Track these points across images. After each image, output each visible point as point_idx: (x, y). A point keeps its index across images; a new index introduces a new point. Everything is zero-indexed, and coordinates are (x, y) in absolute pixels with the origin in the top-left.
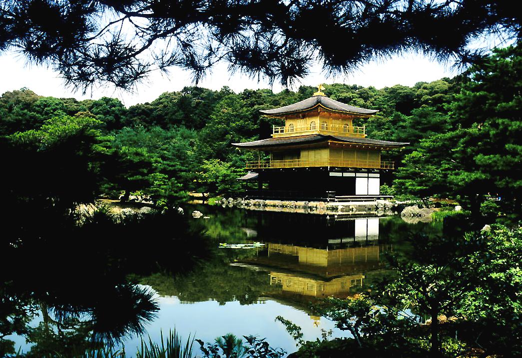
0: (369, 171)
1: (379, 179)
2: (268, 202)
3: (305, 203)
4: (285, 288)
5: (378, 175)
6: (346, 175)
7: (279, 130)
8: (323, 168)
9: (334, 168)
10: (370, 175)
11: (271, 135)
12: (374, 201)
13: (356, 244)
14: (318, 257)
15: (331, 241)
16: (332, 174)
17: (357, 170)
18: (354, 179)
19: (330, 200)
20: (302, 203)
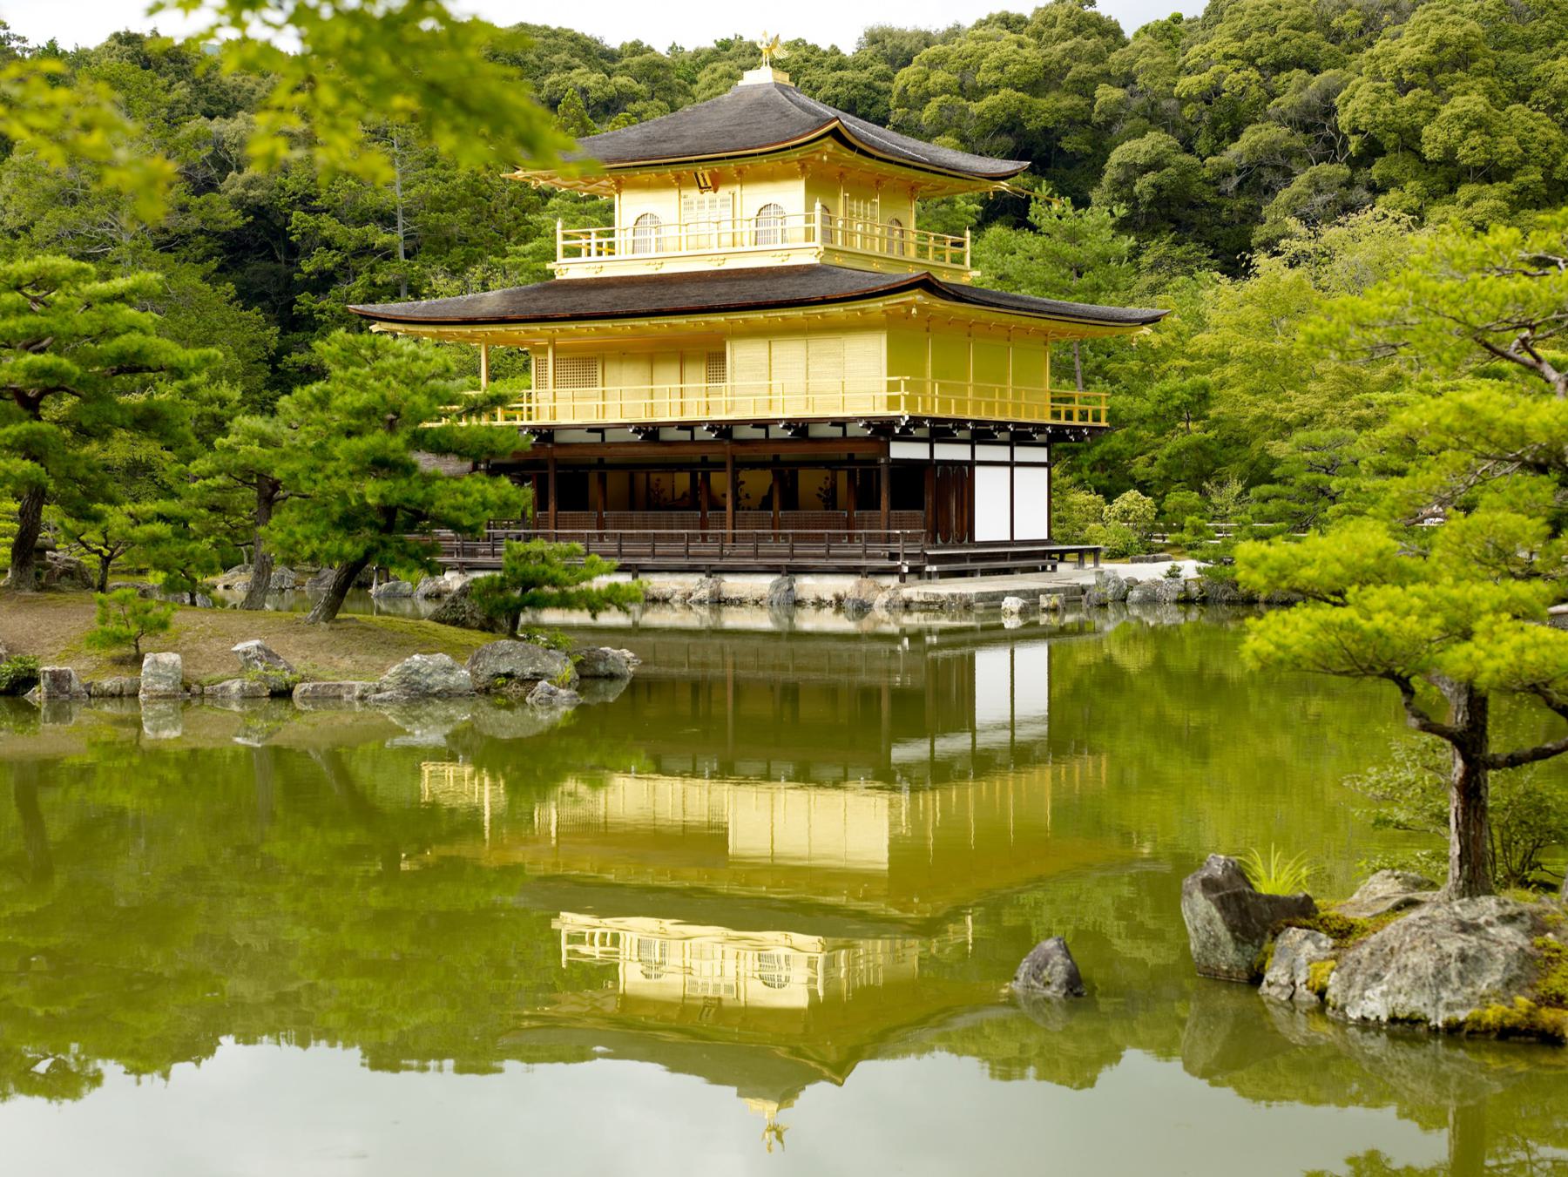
0: (1021, 435)
1: (1045, 470)
3: (776, 587)
4: (632, 977)
5: (1040, 455)
6: (944, 452)
7: (594, 240)
8: (869, 422)
10: (1022, 454)
11: (550, 266)
12: (1044, 569)
13: (982, 763)
14: (841, 825)
15: (901, 753)
16: (899, 451)
17: (983, 433)
18: (972, 464)
19: (912, 570)
20: (763, 584)
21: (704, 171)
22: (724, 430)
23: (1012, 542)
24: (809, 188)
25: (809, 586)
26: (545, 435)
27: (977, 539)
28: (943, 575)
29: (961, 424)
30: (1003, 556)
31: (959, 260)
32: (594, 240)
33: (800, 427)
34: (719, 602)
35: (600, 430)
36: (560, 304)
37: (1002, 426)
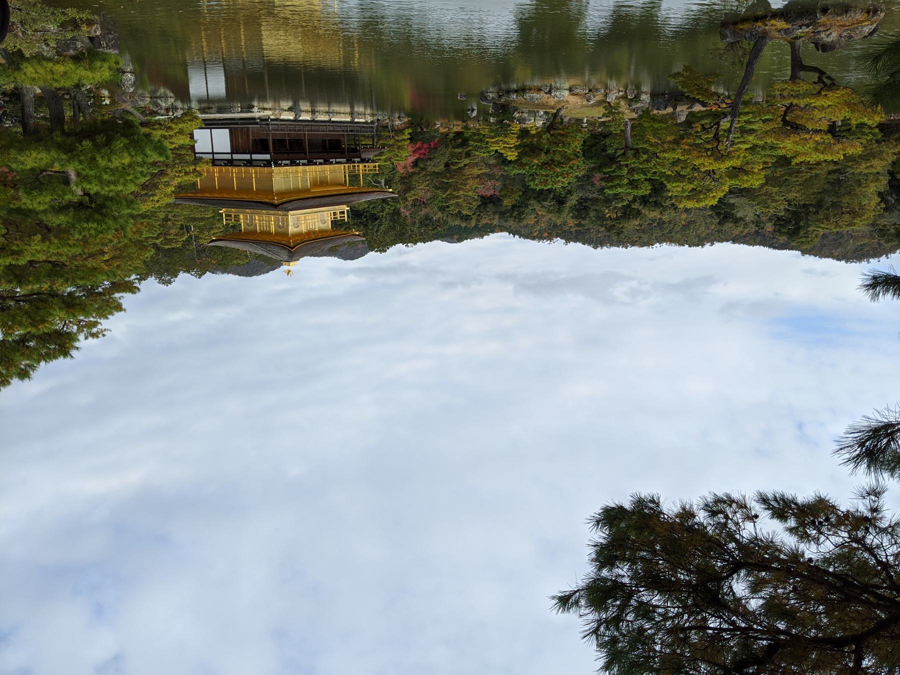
2: (349, 120)
6: (247, 157)
8: (280, 165)
9: (265, 166)
16: (268, 157)
18: (232, 153)
19: (267, 120)
21: (313, 237)
22: (310, 163)
23: (211, 129)
24: (286, 234)
25: (290, 116)
26: (348, 161)
27: (227, 130)
28: (254, 119)
29: (245, 165)
30: (222, 124)
31: (226, 216)
32: (338, 216)
33: (293, 163)
34: (313, 112)
35: (337, 163)
36: (345, 198)
37: (225, 165)
